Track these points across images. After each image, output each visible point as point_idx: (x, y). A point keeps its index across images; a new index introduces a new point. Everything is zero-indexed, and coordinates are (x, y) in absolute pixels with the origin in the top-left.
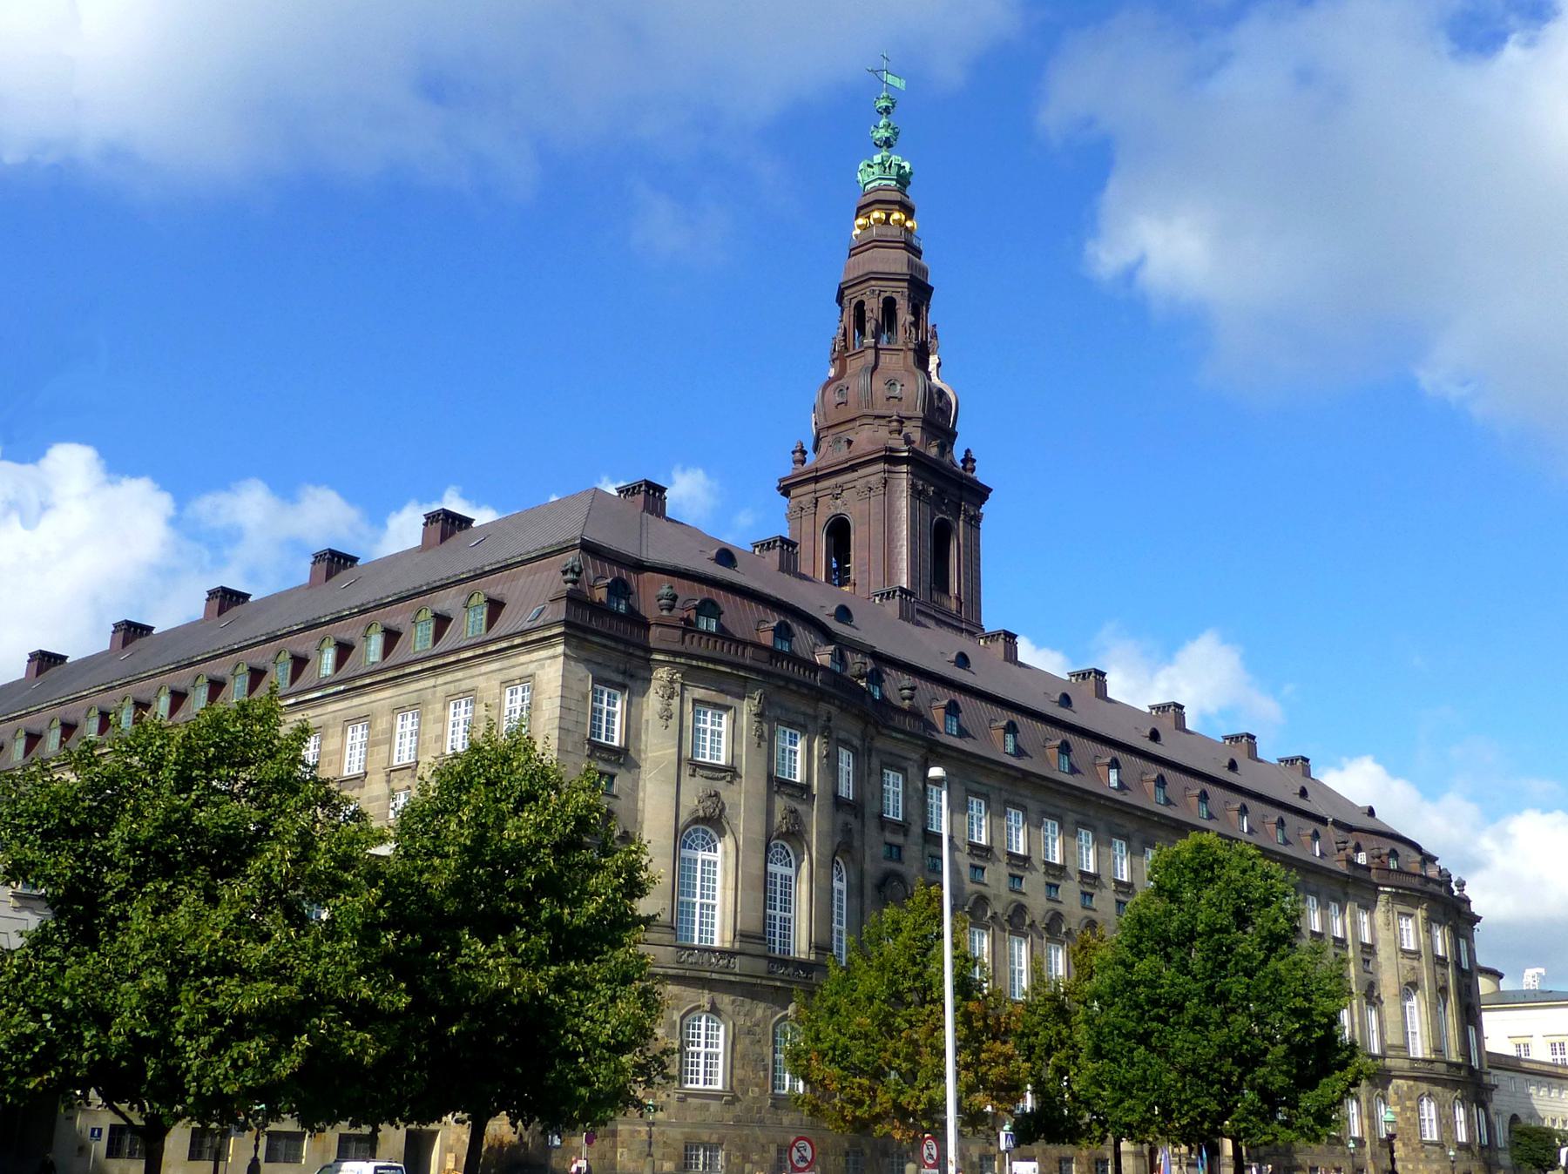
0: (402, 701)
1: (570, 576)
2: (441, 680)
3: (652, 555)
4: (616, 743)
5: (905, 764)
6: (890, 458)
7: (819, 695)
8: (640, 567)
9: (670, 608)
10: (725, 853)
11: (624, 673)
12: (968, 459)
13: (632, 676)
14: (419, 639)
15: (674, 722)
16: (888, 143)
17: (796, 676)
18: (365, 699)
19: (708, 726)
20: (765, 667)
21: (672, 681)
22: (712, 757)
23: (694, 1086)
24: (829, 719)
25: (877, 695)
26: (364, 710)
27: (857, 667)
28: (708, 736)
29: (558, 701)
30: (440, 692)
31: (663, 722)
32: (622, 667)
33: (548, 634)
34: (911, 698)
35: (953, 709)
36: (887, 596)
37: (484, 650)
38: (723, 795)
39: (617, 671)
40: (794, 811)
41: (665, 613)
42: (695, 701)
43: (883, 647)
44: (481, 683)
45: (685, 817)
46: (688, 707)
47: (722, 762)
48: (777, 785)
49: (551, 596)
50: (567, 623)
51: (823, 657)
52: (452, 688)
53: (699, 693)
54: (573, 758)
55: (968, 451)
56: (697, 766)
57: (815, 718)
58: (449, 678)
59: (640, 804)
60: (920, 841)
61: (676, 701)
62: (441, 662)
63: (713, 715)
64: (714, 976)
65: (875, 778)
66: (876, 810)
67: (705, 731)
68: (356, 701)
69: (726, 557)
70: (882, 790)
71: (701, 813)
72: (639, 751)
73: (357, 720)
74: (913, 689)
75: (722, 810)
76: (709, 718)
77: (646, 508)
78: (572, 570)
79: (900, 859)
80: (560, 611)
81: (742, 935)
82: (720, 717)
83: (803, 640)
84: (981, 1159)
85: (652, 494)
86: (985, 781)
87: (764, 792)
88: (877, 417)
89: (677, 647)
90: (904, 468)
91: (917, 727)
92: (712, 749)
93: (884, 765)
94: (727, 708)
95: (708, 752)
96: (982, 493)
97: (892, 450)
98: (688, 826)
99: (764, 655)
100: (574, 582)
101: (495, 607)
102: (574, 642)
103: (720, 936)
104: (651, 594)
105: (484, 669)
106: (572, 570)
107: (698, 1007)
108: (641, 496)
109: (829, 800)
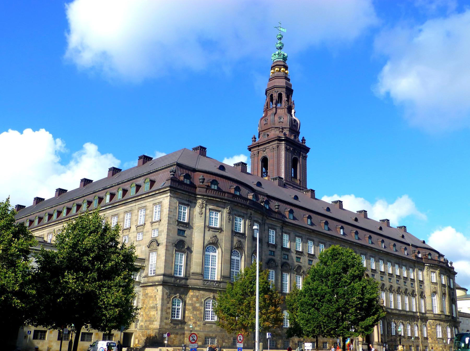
0: (127, 210)
1: (172, 173)
2: (137, 204)
3: (199, 167)
4: (186, 221)
5: (275, 227)
7: (248, 207)
8: (194, 170)
9: (203, 182)
11: (188, 201)
12: (303, 140)
13: (191, 202)
14: (132, 192)
16: (280, 48)
18: (117, 209)
19: (214, 216)
21: (203, 203)
23: (208, 320)
24: (251, 214)
26: (116, 213)
27: (261, 199)
28: (214, 219)
29: (168, 209)
30: (137, 207)
31: (200, 215)
32: (188, 199)
33: (165, 190)
34: (278, 209)
35: (291, 212)
36: (275, 179)
38: (218, 236)
39: (186, 200)
40: (240, 241)
41: (201, 184)
42: (210, 209)
43: (269, 194)
44: (148, 204)
45: (206, 243)
46: (208, 211)
47: (218, 227)
48: (235, 233)
49: (166, 179)
50: (170, 187)
51: (250, 197)
52: (140, 206)
53: (211, 207)
54: (172, 225)
55: (303, 137)
56: (210, 228)
57: (247, 214)
58: (139, 203)
60: (280, 250)
62: (137, 198)
63: (215, 213)
64: (214, 289)
65: (266, 232)
66: (267, 241)
67: (213, 218)
68: (115, 210)
69: (222, 167)
70: (269, 235)
72: (193, 224)
73: (115, 215)
74: (279, 206)
75: (218, 241)
77: (200, 154)
79: (274, 255)
80: (169, 183)
81: (223, 277)
82: (218, 214)
83: (244, 192)
84: (298, 342)
85: (202, 150)
86: (301, 232)
89: (205, 194)
91: (280, 217)
92: (215, 223)
93: (269, 228)
94: (219, 211)
95: (213, 224)
96: (307, 150)
97: (280, 137)
98: (207, 245)
99: (231, 196)
100: (173, 175)
101: (152, 183)
102: (173, 192)
103: (217, 277)
104: (197, 178)
105: (149, 200)
106: (173, 171)
107: (210, 297)
108: (199, 151)
109: (251, 238)
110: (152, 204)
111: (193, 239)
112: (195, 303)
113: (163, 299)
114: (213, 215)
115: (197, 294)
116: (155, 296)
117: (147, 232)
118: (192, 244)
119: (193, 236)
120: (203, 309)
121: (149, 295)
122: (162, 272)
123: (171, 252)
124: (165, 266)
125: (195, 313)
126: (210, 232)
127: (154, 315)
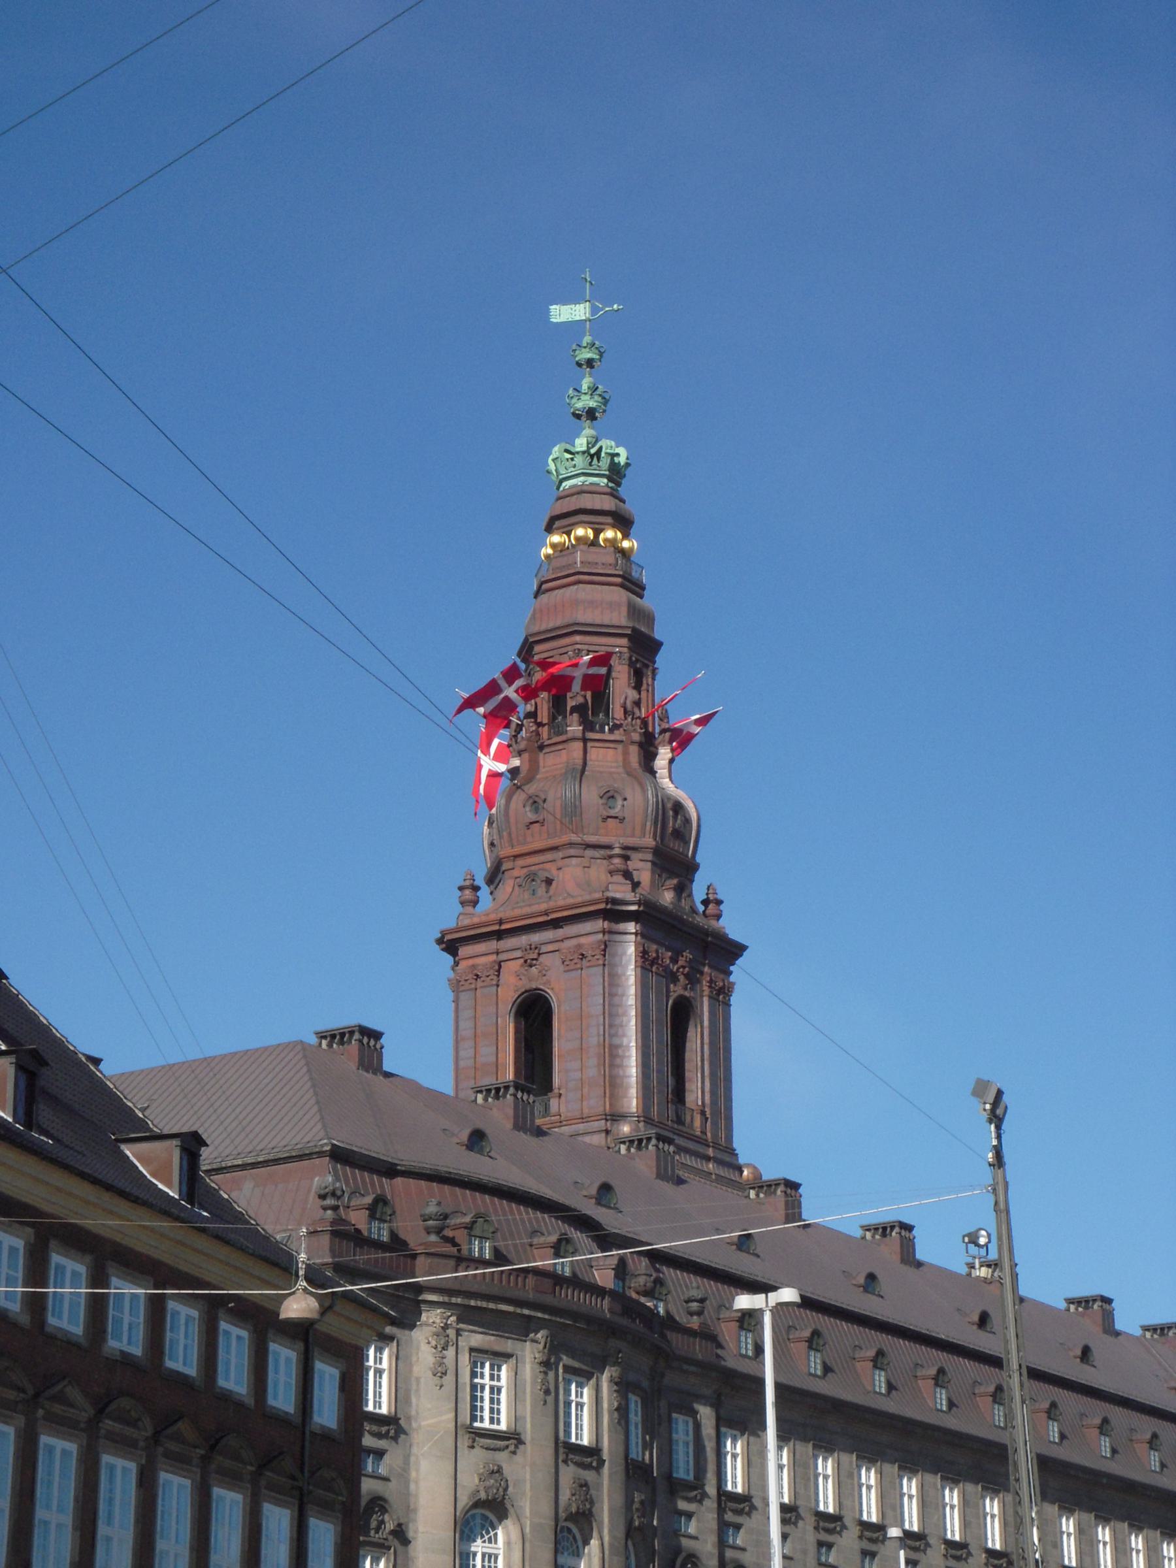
1: (330, 1202)
6: (613, 913)
15: (449, 1379)
19: (487, 1380)
21: (446, 1327)
22: (492, 1421)
31: (436, 1380)
40: (584, 1485)
46: (465, 1359)
47: (503, 1426)
53: (477, 1339)
61: (451, 1352)
67: (483, 1387)
72: (409, 1418)
87: (551, 1461)
88: (589, 846)
90: (631, 927)
94: (507, 1356)
106: (333, 1194)
111: (412, 1486)
114: (482, 1377)
118: (410, 1510)
119: (413, 1474)
126: (477, 1451)
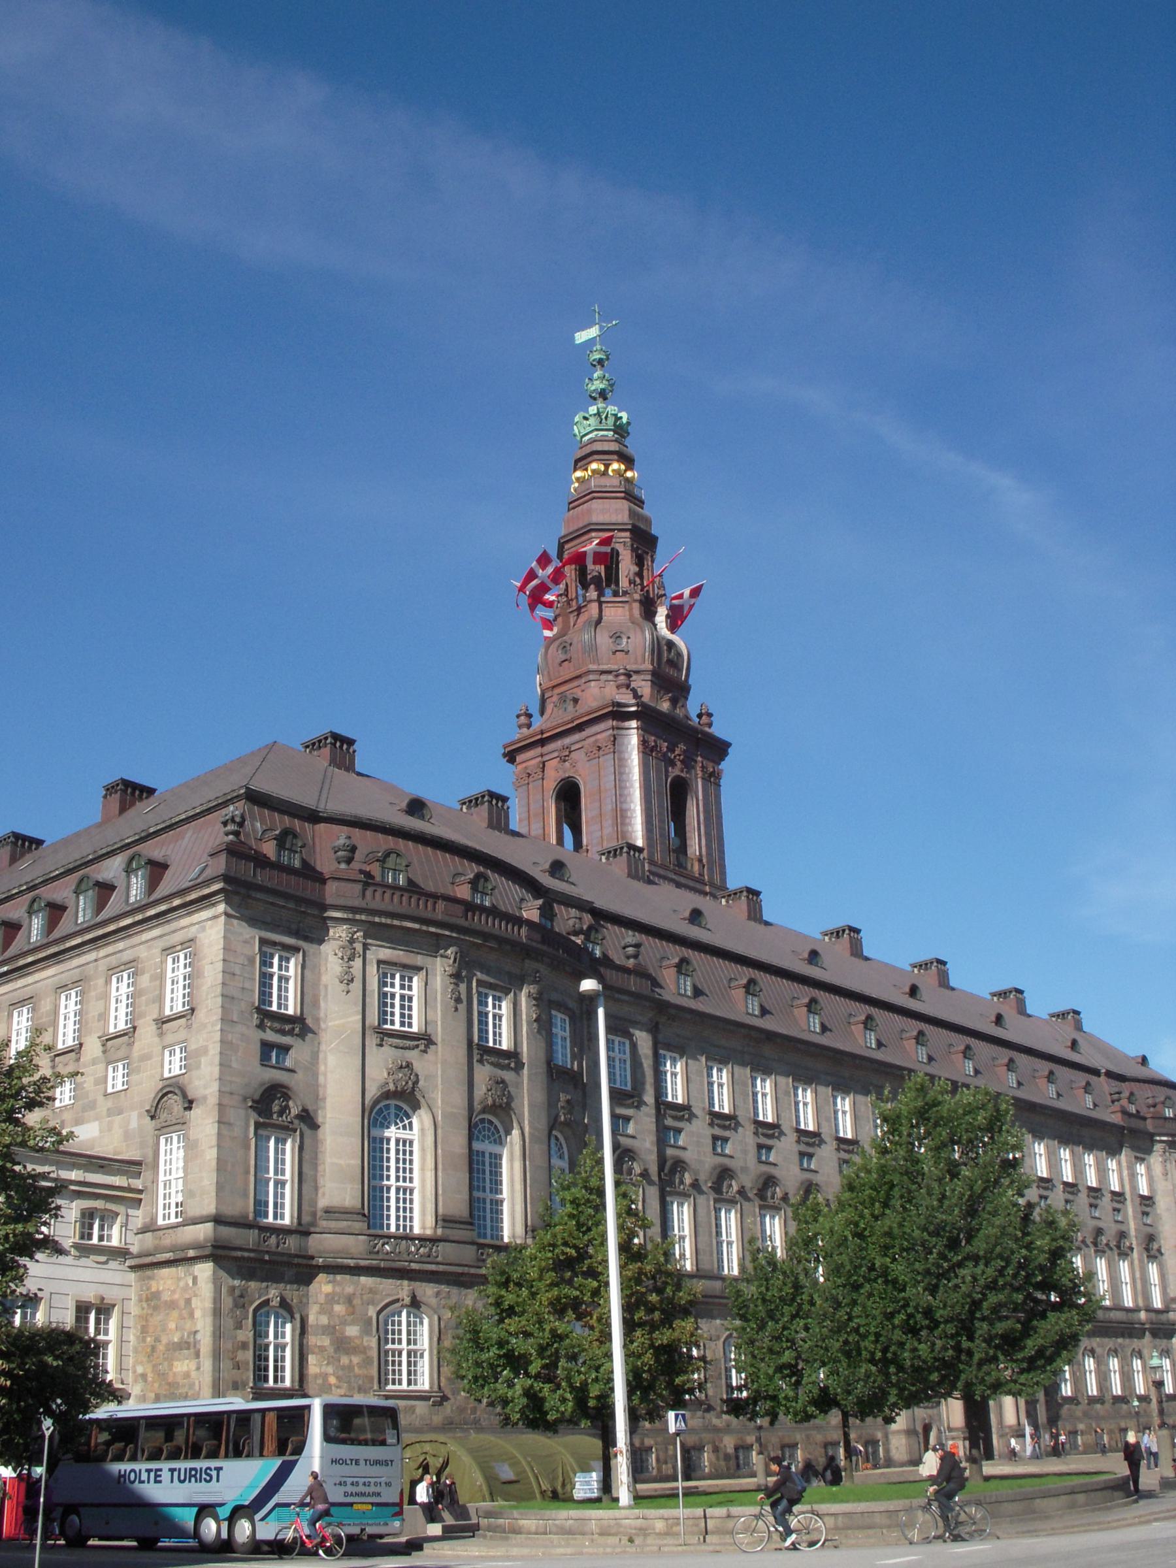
0: (65, 978)
2: (102, 953)
3: (333, 805)
4: (291, 1012)
7: (525, 952)
8: (314, 817)
9: (349, 861)
10: (422, 1130)
14: (82, 910)
15: (357, 986)
16: (603, 395)
17: (496, 932)
18: (29, 980)
20: (462, 922)
21: (352, 941)
22: (402, 1024)
23: (397, 1387)
25: (598, 953)
26: (28, 992)
27: (571, 922)
28: (397, 1001)
29: (220, 966)
30: (102, 966)
31: (343, 986)
33: (206, 891)
34: (636, 956)
35: (682, 966)
36: (613, 853)
37: (148, 916)
38: (417, 1066)
41: (343, 866)
42: (379, 962)
43: (600, 903)
44: (142, 952)
45: (372, 1091)
46: (372, 970)
47: (415, 1029)
48: (479, 1051)
49: (209, 850)
50: (226, 878)
51: (531, 912)
52: (113, 960)
53: (386, 953)
54: (240, 1028)
56: (384, 1035)
58: (110, 949)
59: (321, 1079)
61: (358, 963)
62: (100, 932)
63: (402, 978)
64: (414, 1266)
67: (393, 996)
68: (20, 983)
69: (416, 807)
71: (392, 1087)
73: (21, 1003)
74: (637, 946)
75: (416, 1082)
76: (397, 981)
77: (333, 762)
78: (233, 820)
80: (220, 865)
81: (444, 1220)
82: (410, 980)
83: (506, 894)
84: (736, 1449)
85: (340, 748)
87: (464, 1060)
89: (357, 903)
91: (644, 987)
92: (402, 1015)
95: (397, 1018)
97: (619, 705)
98: (376, 1102)
99: (459, 909)
100: (236, 834)
101: (157, 869)
102: (236, 899)
103: (421, 1223)
104: (325, 847)
105: (146, 936)
107: (397, 1301)
108: (326, 751)
109: (542, 1069)
110: (156, 951)
112: (344, 1323)
113: (217, 1312)
114: (393, 985)
115: (349, 1289)
116: (188, 1301)
117: (146, 1057)
118: (317, 1098)
120: (374, 1343)
121: (166, 1297)
122: (209, 1207)
123: (237, 1131)
124: (220, 1187)
125: (345, 1360)
127: (187, 1375)
